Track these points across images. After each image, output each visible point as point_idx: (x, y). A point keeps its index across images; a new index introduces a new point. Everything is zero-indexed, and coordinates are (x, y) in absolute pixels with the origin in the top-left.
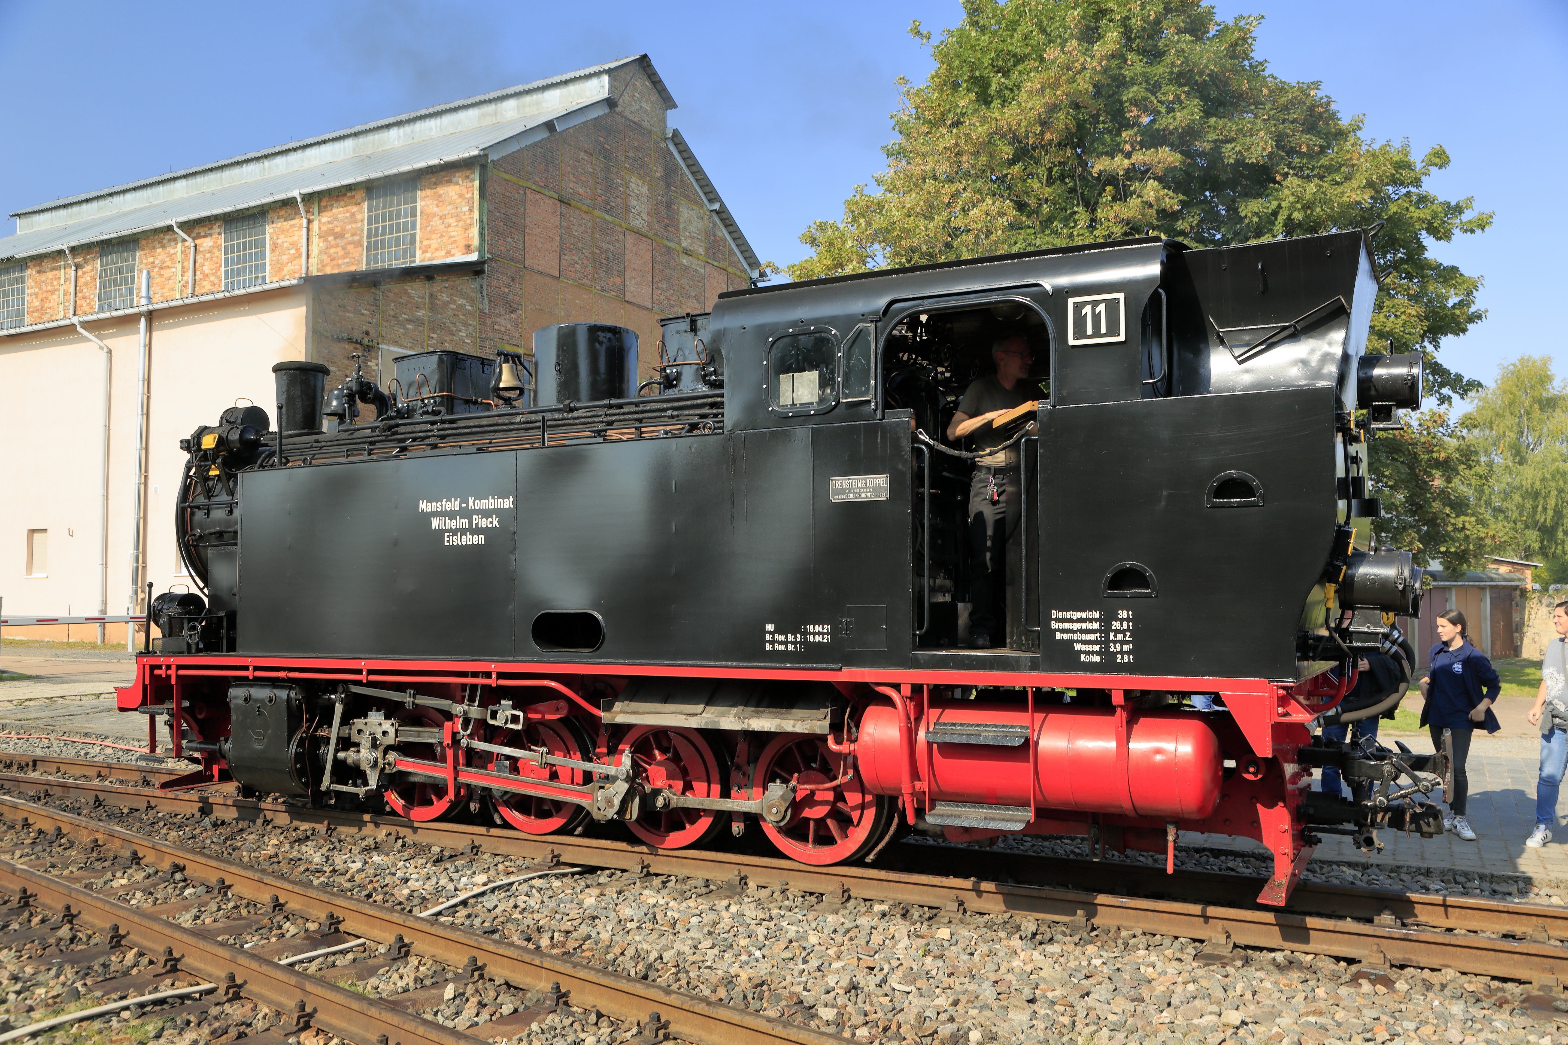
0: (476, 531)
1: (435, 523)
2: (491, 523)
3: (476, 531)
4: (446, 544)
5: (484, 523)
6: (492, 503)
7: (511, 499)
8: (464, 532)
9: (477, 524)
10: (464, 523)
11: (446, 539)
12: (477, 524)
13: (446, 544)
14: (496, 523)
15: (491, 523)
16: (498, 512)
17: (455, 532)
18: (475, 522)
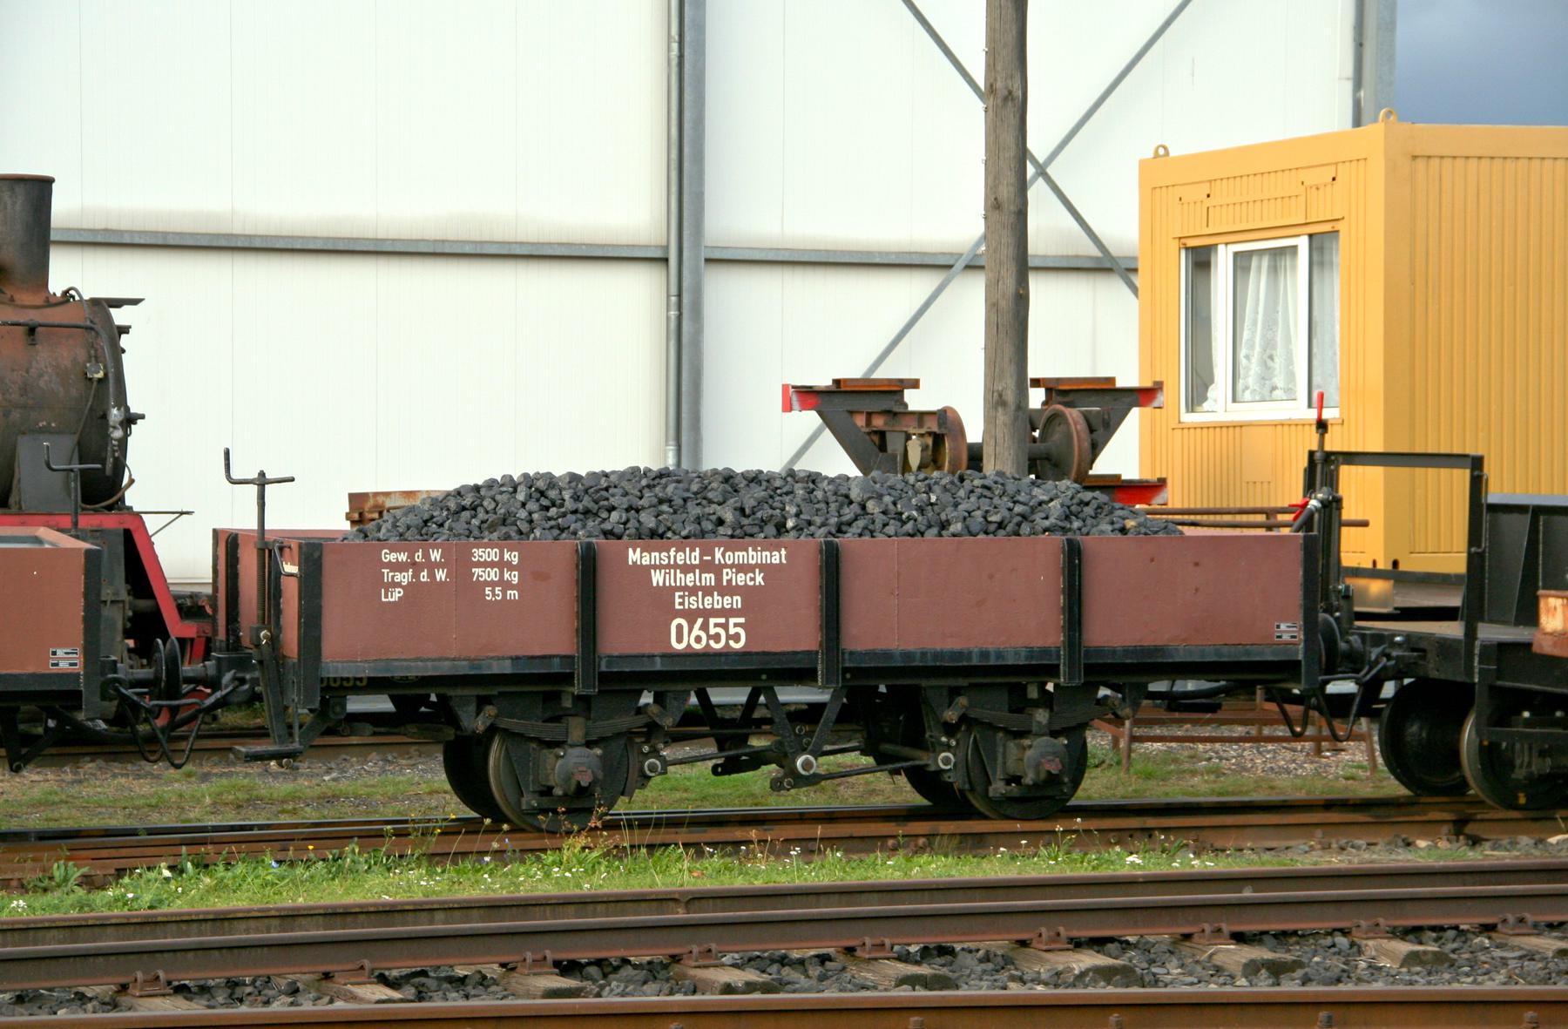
0: (730, 590)
1: (657, 578)
2: (752, 579)
3: (730, 590)
4: (677, 607)
5: (741, 579)
6: (752, 556)
7: (783, 552)
8: (708, 591)
9: (729, 581)
10: (709, 579)
11: (678, 600)
12: (729, 581)
13: (677, 607)
14: (759, 579)
15: (752, 579)
16: (763, 567)
17: (693, 591)
18: (725, 578)
